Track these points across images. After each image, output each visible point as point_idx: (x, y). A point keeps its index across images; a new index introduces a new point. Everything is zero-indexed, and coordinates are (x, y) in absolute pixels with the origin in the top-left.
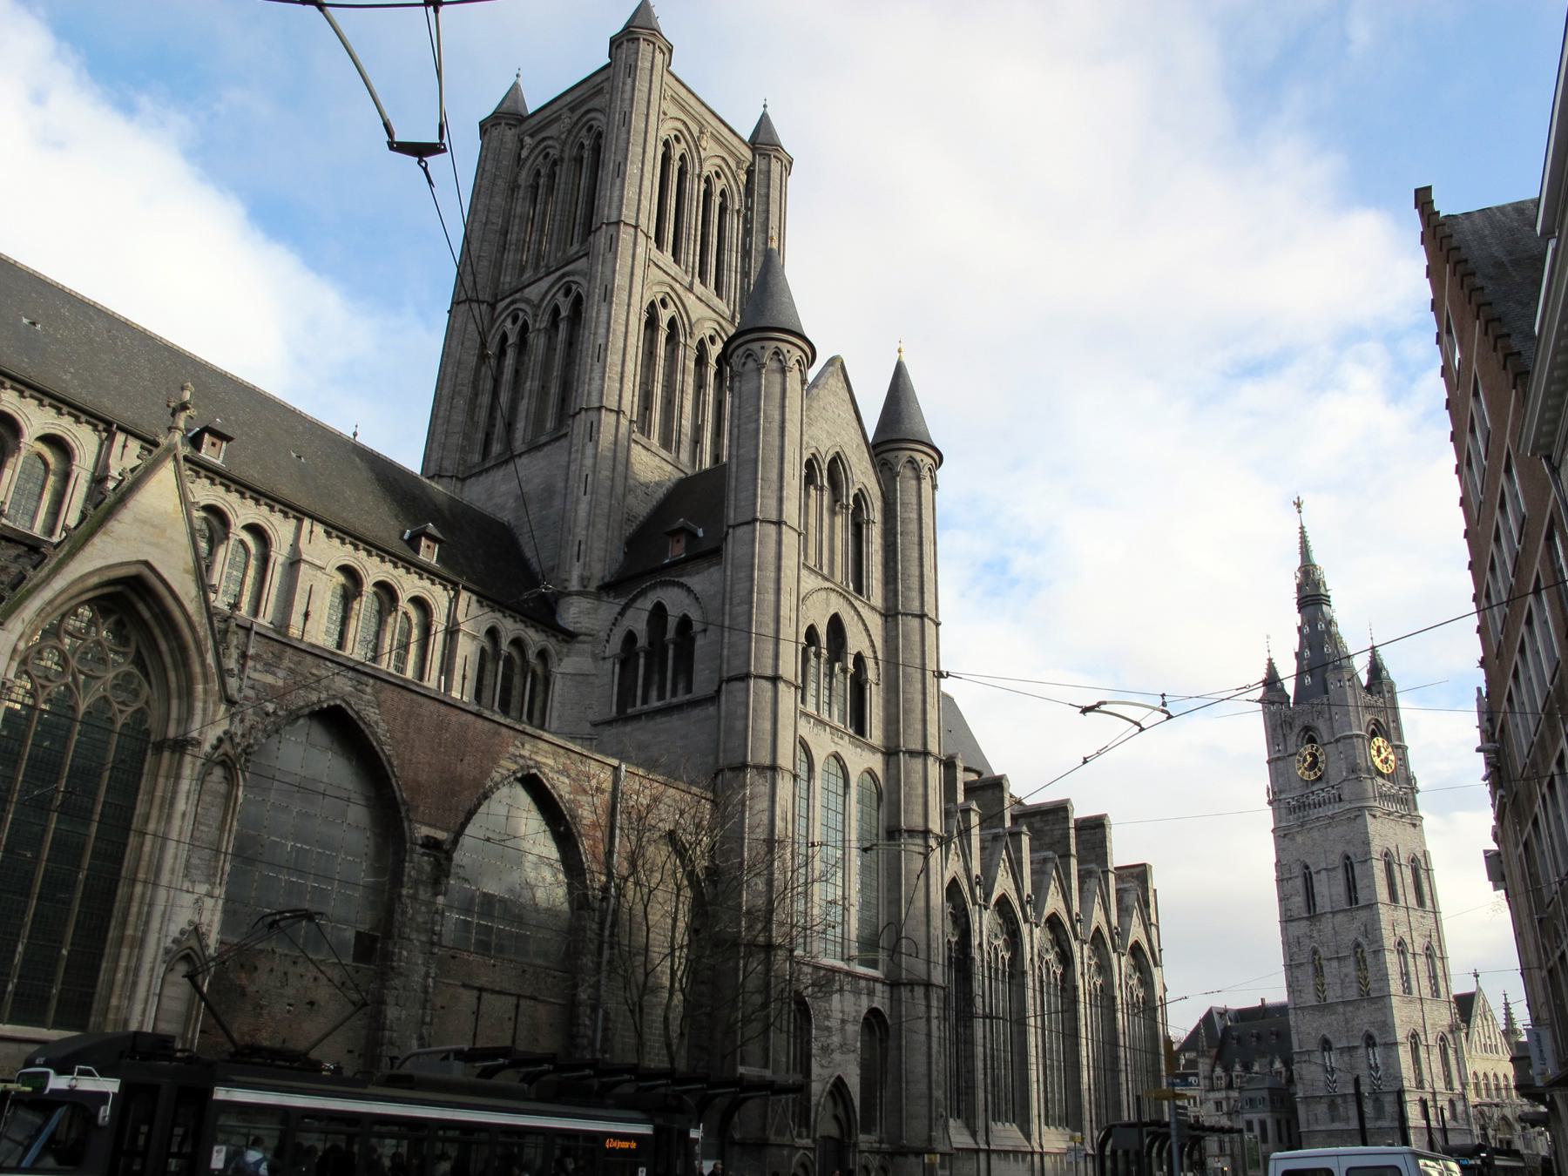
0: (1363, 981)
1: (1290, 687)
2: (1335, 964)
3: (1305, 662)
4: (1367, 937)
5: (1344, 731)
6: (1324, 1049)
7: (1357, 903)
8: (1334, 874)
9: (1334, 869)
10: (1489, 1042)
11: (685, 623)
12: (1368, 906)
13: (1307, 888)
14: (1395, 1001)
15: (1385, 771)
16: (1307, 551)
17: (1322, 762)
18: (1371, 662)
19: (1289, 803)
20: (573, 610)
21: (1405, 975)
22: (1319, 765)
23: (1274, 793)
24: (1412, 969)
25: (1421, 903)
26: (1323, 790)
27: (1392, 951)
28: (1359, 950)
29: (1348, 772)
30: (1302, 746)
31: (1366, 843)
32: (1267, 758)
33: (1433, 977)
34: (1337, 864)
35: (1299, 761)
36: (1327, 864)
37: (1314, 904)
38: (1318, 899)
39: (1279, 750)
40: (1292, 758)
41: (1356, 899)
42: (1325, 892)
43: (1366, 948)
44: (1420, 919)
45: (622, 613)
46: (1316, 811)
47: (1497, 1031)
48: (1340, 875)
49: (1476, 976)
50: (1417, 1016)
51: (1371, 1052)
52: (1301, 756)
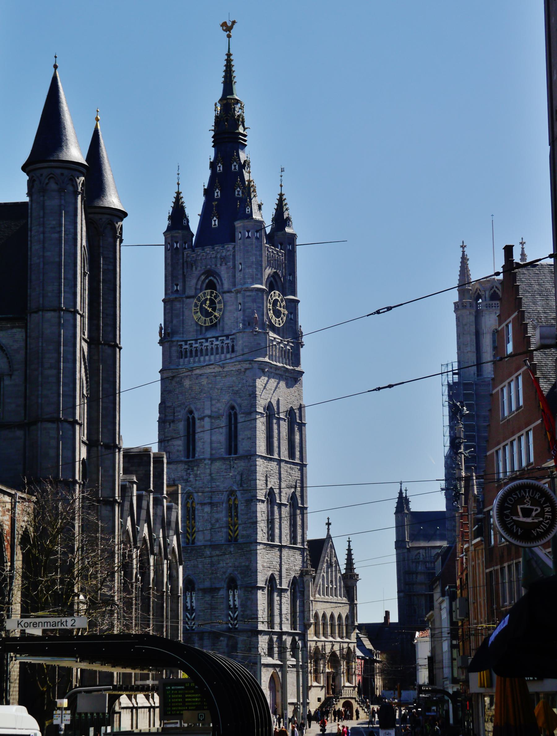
0: (232, 526)
1: (194, 226)
2: (207, 509)
3: (214, 203)
4: (241, 486)
5: (245, 283)
7: (236, 453)
10: (331, 586)
12: (247, 456)
15: (277, 325)
16: (231, 81)
18: (276, 210)
19: (181, 345)
25: (292, 454)
26: (217, 338)
27: (263, 502)
29: (244, 324)
31: (253, 396)
32: (163, 297)
35: (196, 305)
36: (211, 411)
38: (199, 445)
39: (177, 290)
40: (188, 300)
41: (236, 446)
46: (207, 358)
47: (339, 575)
49: (329, 524)
52: (199, 300)
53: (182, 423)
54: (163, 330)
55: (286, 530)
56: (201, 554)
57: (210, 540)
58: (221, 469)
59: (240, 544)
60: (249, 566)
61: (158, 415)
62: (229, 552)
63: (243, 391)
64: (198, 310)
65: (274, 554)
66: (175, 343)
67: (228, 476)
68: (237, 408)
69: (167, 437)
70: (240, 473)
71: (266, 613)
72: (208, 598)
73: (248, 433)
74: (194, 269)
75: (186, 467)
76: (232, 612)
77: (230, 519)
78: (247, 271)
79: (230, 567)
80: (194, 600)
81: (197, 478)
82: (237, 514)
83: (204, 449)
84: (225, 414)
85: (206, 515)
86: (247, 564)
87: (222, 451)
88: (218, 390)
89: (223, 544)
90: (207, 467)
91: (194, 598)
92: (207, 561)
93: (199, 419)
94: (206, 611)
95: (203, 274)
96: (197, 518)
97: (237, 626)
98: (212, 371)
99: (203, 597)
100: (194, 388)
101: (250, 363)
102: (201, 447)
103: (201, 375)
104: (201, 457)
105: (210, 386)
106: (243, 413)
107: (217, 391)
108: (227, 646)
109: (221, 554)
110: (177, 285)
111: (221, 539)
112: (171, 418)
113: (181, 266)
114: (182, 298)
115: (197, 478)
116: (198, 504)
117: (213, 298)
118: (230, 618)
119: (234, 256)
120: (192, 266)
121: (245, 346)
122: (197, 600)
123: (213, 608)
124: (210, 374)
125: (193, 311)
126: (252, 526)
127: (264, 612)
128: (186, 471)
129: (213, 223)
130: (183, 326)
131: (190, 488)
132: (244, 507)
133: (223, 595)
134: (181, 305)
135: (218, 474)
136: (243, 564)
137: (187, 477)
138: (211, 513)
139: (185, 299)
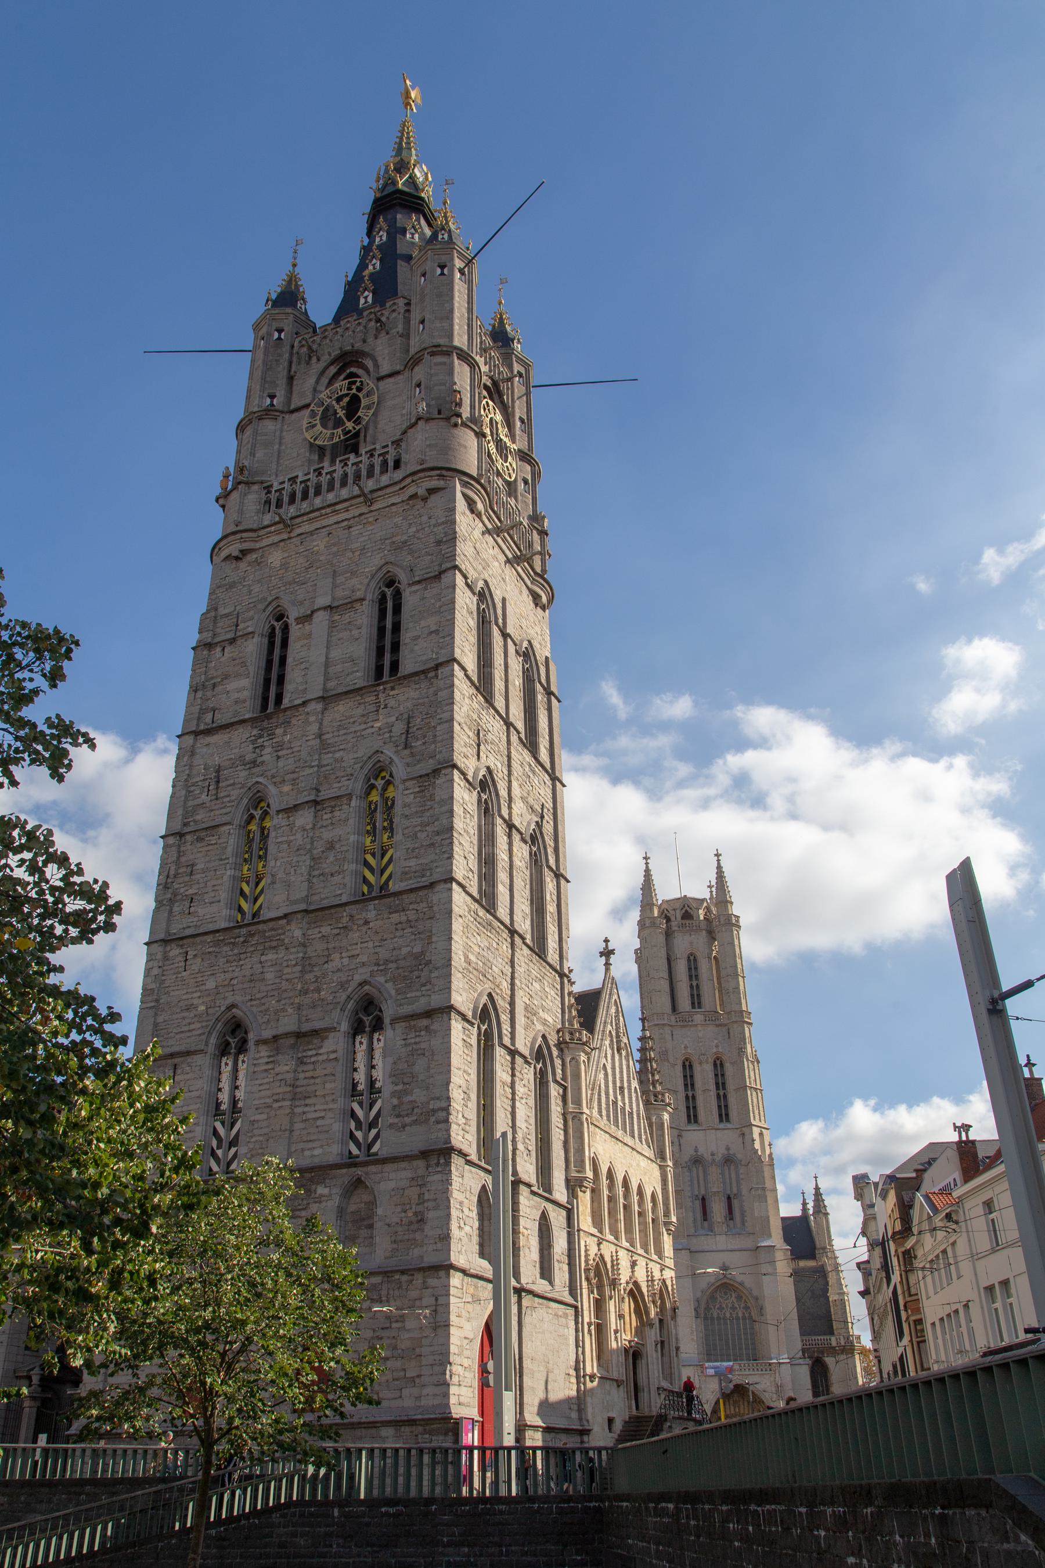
2: (304, 818)
6: (224, 1050)
8: (346, 618)
9: (351, 604)
12: (423, 672)
13: (269, 663)
14: (458, 897)
17: (369, 407)
21: (487, 862)
23: (241, 469)
24: (502, 856)
28: (380, 783)
32: (242, 416)
34: (359, 595)
35: (313, 414)
36: (334, 599)
39: (272, 405)
43: (400, 771)
44: (527, 769)
48: (365, 618)
50: (500, 966)
51: (361, 1049)
53: (256, 639)
54: (231, 478)
55: (523, 907)
56: (274, 944)
57: (306, 899)
58: (351, 717)
59: (396, 894)
60: (422, 953)
61: (197, 636)
62: (361, 922)
63: (418, 539)
64: (318, 422)
65: (495, 945)
66: (255, 487)
67: (373, 730)
68: (403, 577)
69: (212, 678)
70: (406, 716)
71: (473, 1104)
72: (285, 1066)
73: (431, 622)
74: (314, 360)
75: (255, 732)
76: (361, 1104)
77: (368, 840)
78: (438, 325)
79: (364, 964)
80: (241, 1081)
81: (280, 753)
82: (391, 822)
83: (306, 683)
84: (369, 597)
85: (299, 836)
86: (417, 949)
87: (359, 677)
88: (353, 552)
89: (346, 904)
90: (312, 719)
91: (241, 1075)
92: (292, 957)
94: (276, 1105)
95: (332, 363)
96: (272, 848)
97: (374, 1149)
98: (345, 516)
99: (270, 1066)
100: (292, 564)
101: (441, 476)
102: (300, 680)
103: (311, 533)
104: (299, 702)
105: (335, 549)
106: (419, 582)
107: (350, 554)
108: (341, 1212)
109: (338, 931)
110: (272, 397)
111: (339, 892)
113: (286, 364)
114: (282, 412)
115: (280, 753)
116: (278, 812)
117: (354, 391)
118: (353, 1125)
120: (310, 357)
121: (429, 446)
122: (252, 1076)
123: (297, 1095)
124: (334, 526)
125: (305, 426)
126: (438, 838)
127: (469, 1099)
128: (253, 742)
129: (362, 301)
130: (278, 463)
131: (260, 779)
132: (412, 796)
133: (335, 1052)
134: (279, 426)
135: (342, 732)
136: (405, 951)
137: (255, 755)
138: (313, 828)
139: (287, 416)
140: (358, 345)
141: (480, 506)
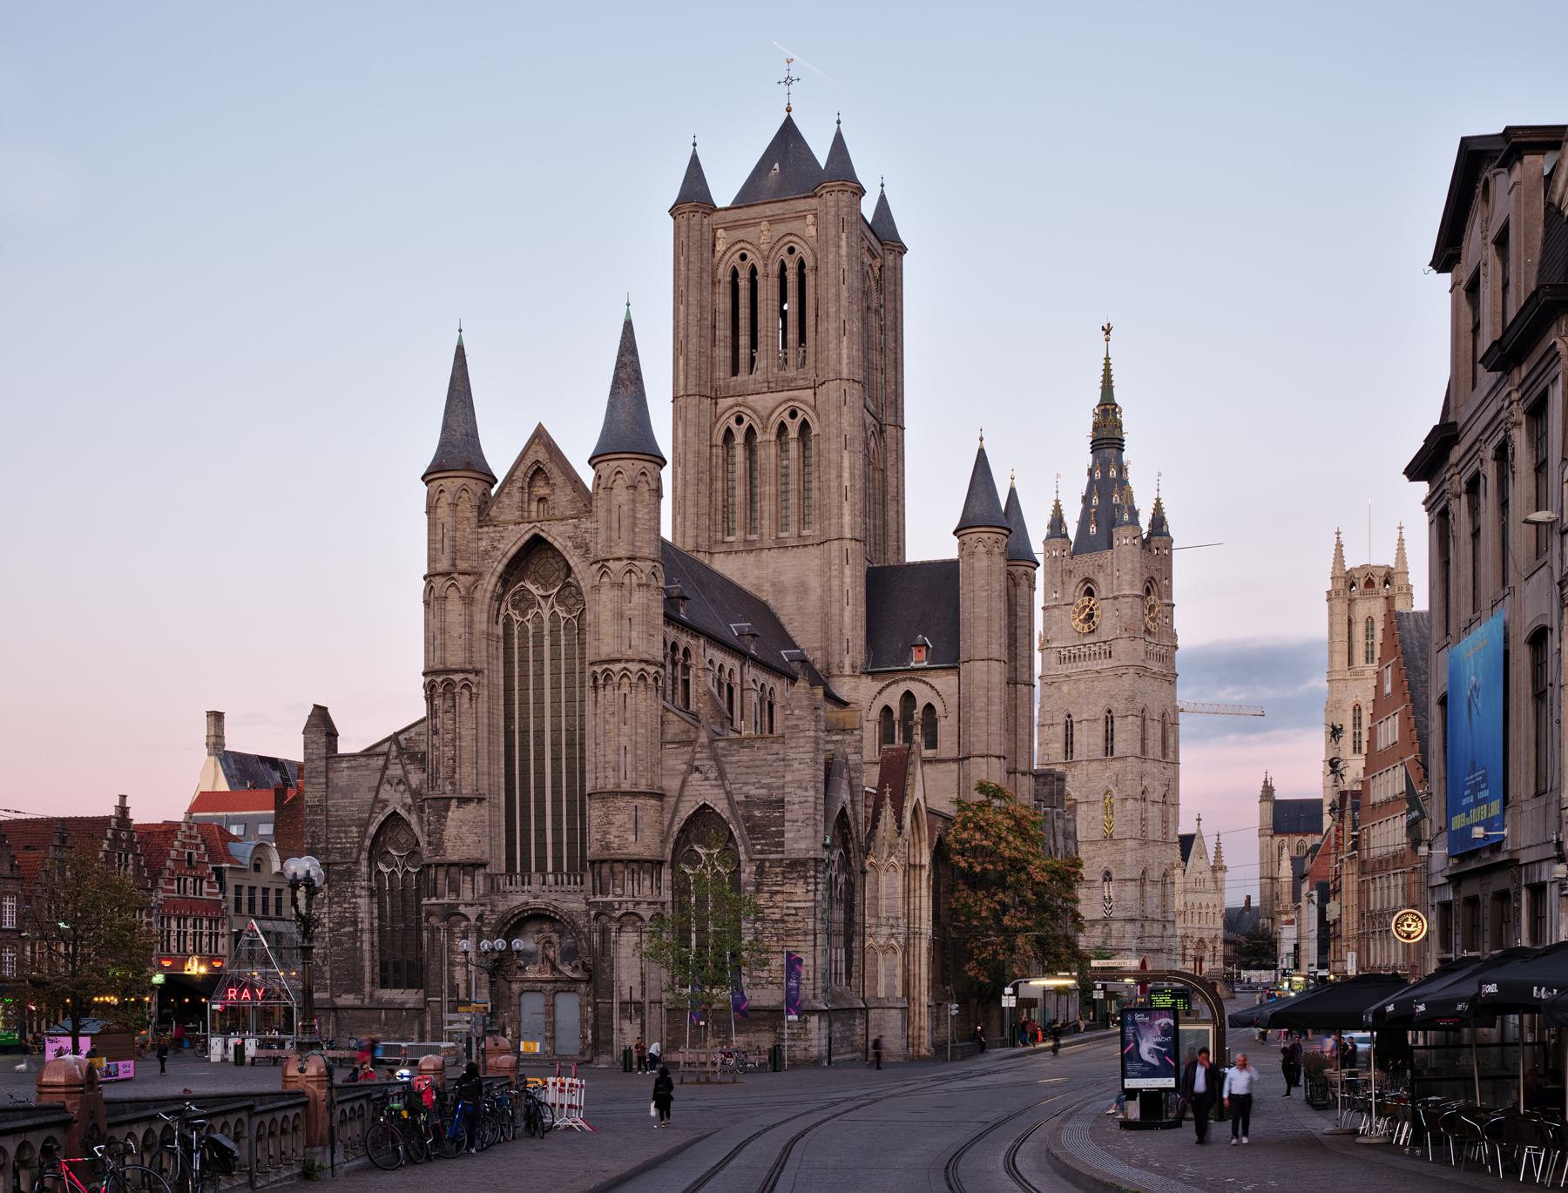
7: (1112, 754)
8: (1095, 725)
11: (929, 708)
13: (1067, 735)
17: (1098, 616)
20: (846, 687)
22: (1094, 619)
25: (1164, 755)
30: (1079, 597)
33: (1165, 821)
37: (1072, 751)
38: (1076, 746)
41: (1112, 747)
42: (1084, 741)
45: (880, 693)
48: (1101, 726)
49: (1199, 820)
87: (1100, 754)
93: (1077, 722)
110: (1056, 592)
112: (1050, 722)
119: (1112, 563)
140: (1090, 577)
141: (1142, 673)
